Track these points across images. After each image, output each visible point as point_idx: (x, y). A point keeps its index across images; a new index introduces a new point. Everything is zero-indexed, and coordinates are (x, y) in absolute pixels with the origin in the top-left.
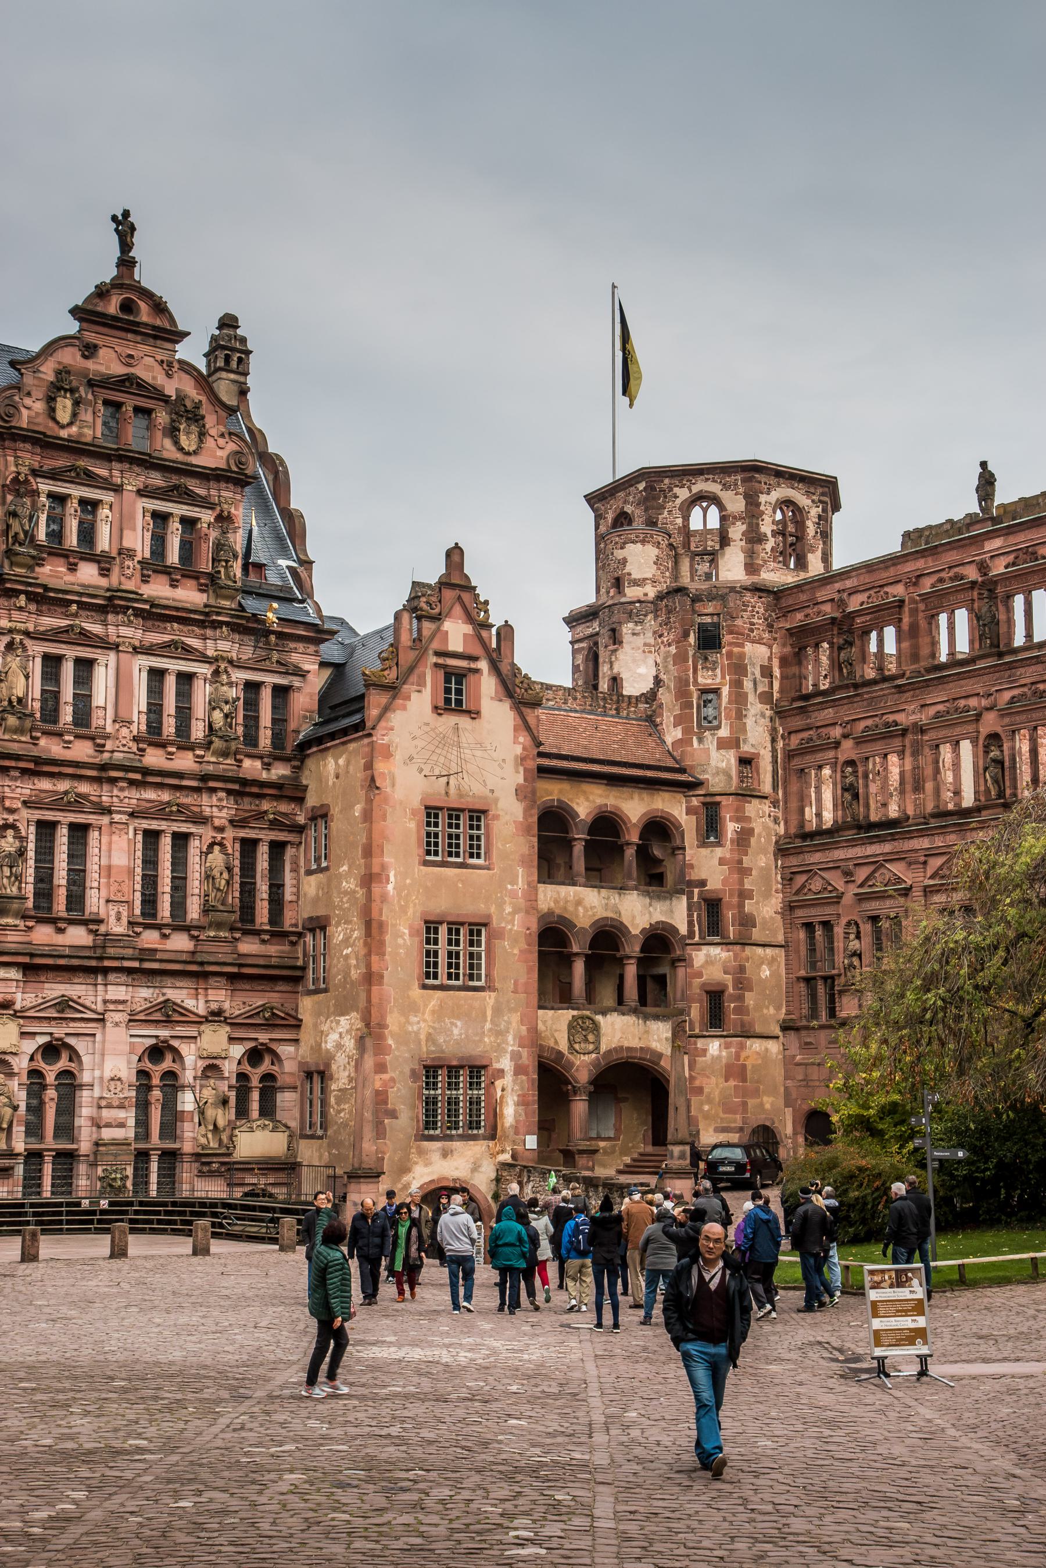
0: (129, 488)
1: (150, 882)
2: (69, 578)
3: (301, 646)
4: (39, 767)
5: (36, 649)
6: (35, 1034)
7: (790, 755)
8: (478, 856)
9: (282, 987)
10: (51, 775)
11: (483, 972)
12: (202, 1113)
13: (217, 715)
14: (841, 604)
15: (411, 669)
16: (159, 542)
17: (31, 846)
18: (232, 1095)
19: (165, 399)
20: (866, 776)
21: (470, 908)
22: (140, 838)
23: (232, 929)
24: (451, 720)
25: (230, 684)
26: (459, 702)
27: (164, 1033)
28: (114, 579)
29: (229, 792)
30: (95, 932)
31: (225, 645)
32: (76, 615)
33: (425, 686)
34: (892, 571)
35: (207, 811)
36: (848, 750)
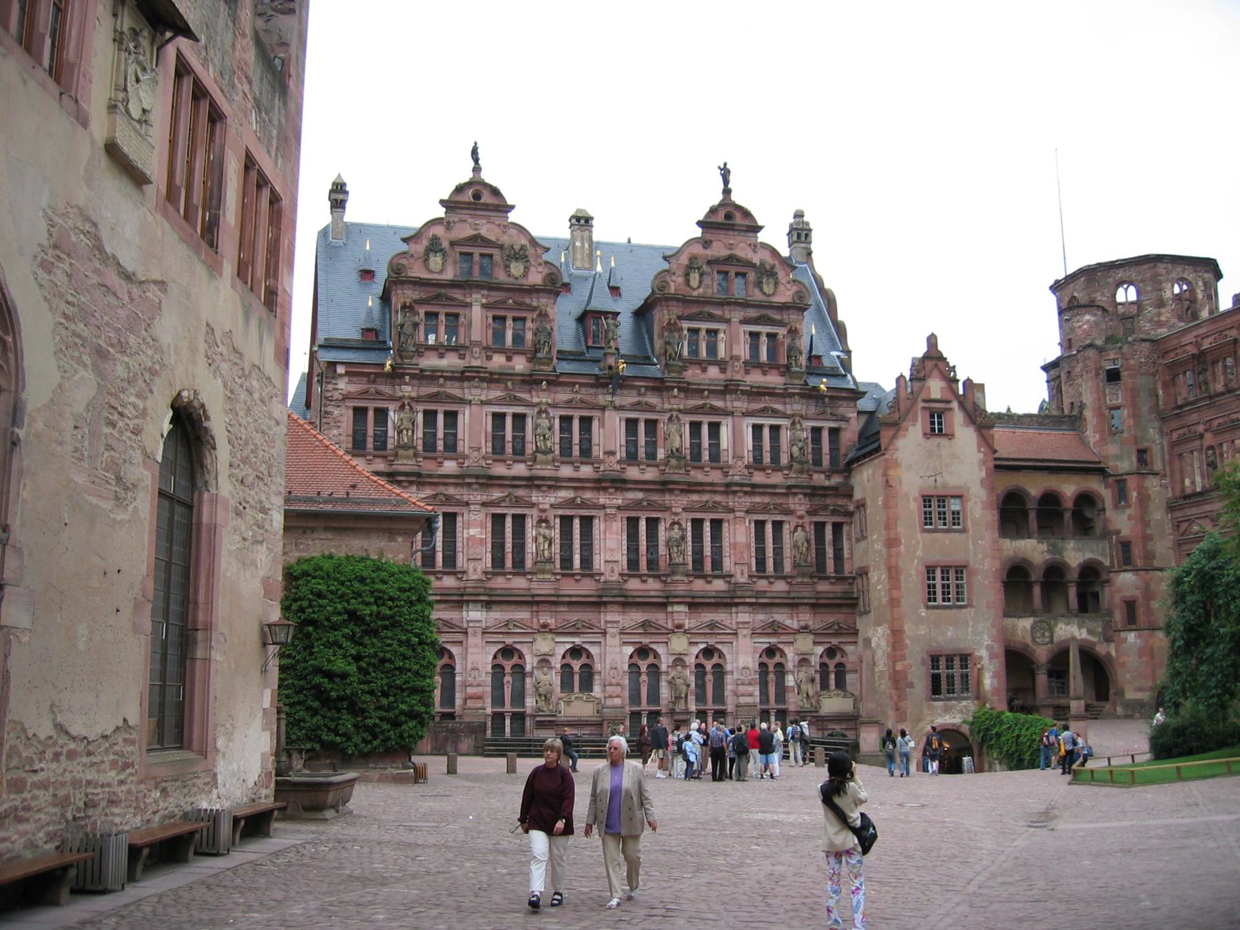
1: (761, 551)
2: (703, 376)
3: (844, 403)
5: (687, 419)
6: (697, 643)
7: (1173, 445)
9: (845, 610)
11: (966, 596)
12: (799, 687)
13: (795, 449)
14: (1197, 345)
15: (908, 412)
16: (755, 348)
17: (689, 534)
18: (818, 677)
19: (753, 266)
20: (1222, 455)
21: (956, 558)
22: (753, 525)
23: (812, 577)
24: (937, 440)
25: (802, 430)
26: (940, 430)
27: (773, 640)
28: (729, 375)
29: (805, 495)
30: (729, 582)
31: (796, 407)
32: (708, 397)
34: (1228, 321)
35: (792, 507)
36: (1209, 439)
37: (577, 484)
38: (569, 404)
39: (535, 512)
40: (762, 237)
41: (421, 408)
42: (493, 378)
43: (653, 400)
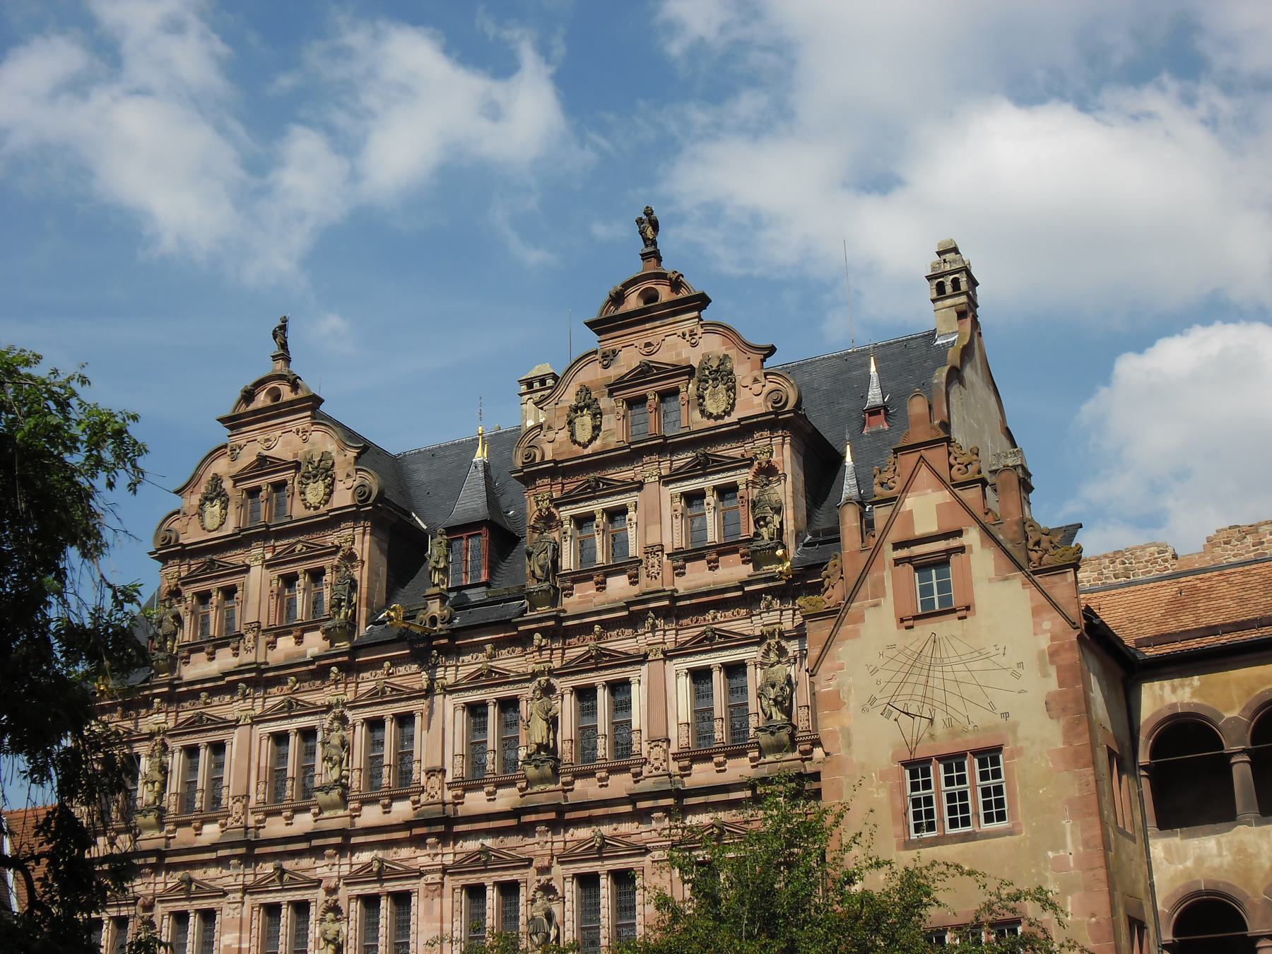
0: (651, 480)
4: (561, 818)
8: (1001, 817)
10: (588, 822)
19: (690, 371)
26: (945, 600)
28: (645, 584)
33: (884, 594)
37: (385, 836)
38: (377, 697)
39: (320, 894)
40: (707, 315)
41: (175, 744)
42: (260, 678)
43: (511, 662)
